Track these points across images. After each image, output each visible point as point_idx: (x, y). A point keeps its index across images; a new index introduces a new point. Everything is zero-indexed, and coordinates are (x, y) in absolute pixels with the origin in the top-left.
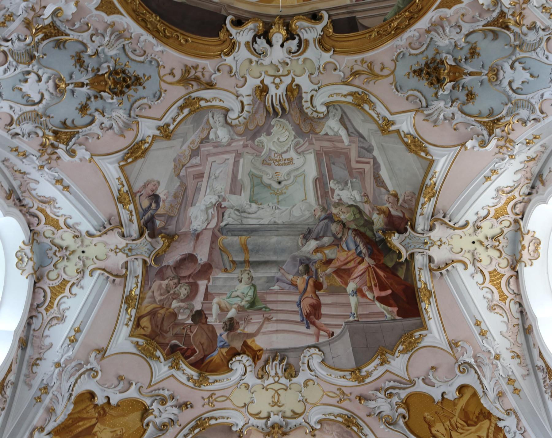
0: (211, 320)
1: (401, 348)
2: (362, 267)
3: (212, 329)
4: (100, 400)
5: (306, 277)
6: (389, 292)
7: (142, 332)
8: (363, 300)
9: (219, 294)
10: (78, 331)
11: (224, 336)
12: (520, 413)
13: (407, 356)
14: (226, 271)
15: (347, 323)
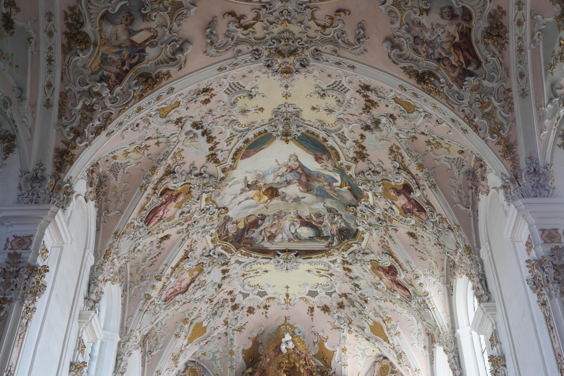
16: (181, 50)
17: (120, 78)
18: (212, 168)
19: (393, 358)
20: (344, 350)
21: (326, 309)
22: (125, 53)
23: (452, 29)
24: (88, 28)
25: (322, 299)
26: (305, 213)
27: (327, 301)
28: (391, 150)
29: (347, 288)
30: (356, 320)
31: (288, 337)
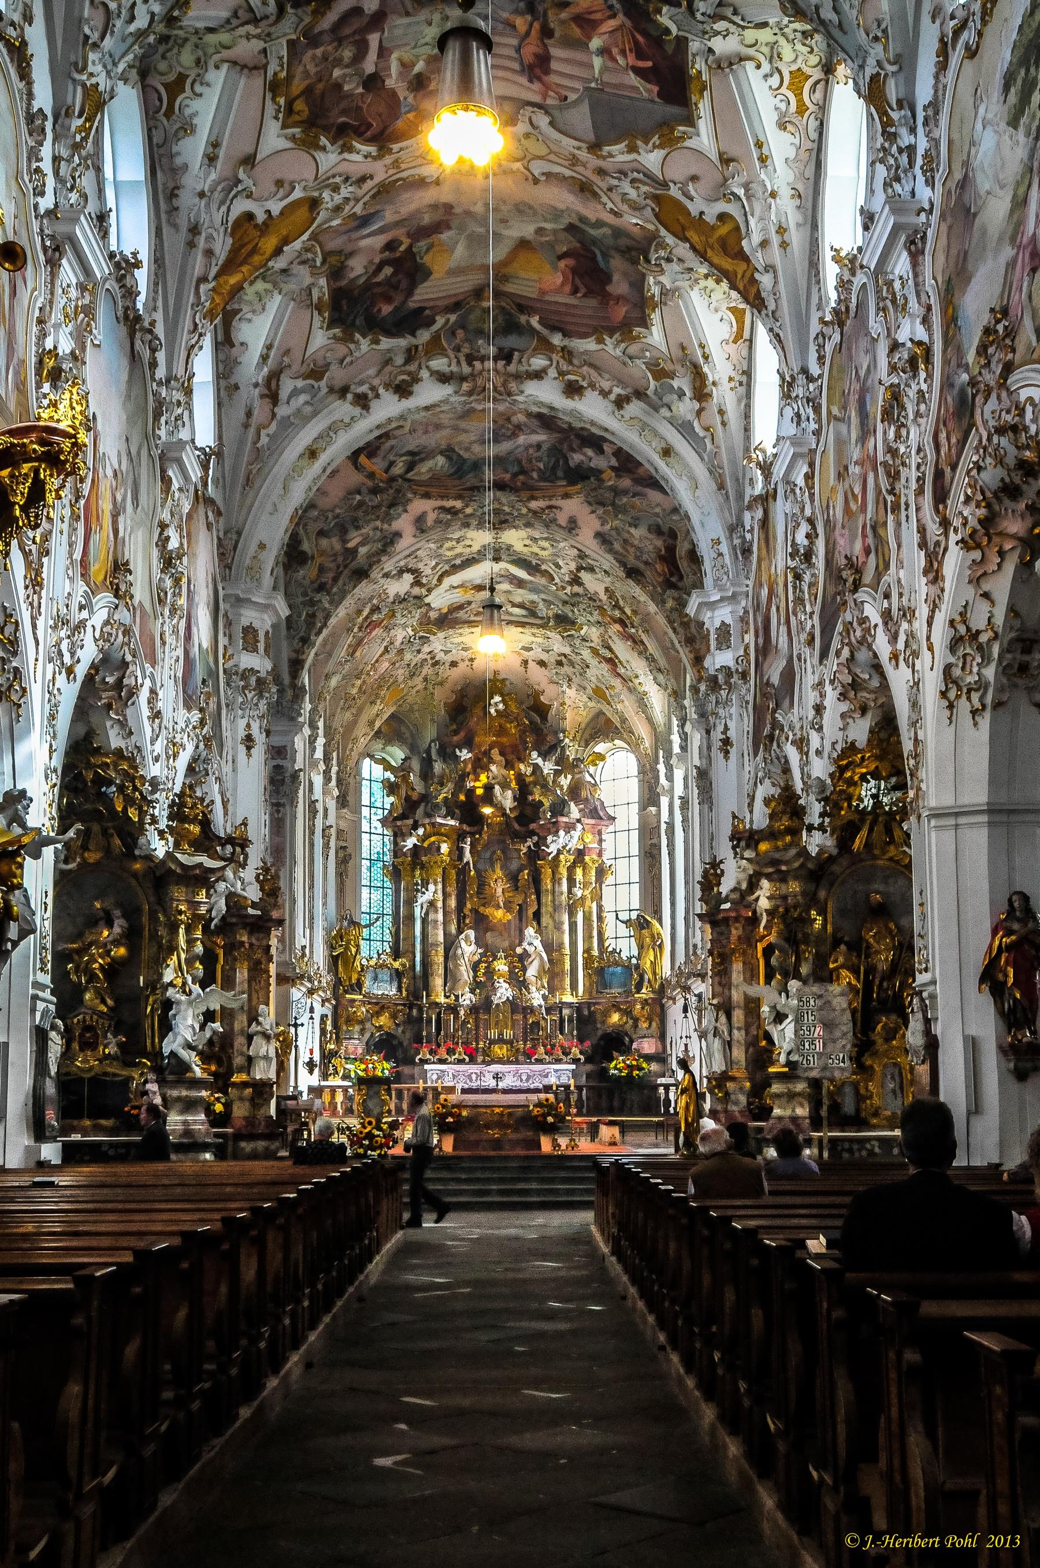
0: (390, 83)
1: (656, 139)
2: (612, 24)
3: (393, 94)
4: (261, 217)
5: (529, 18)
6: (650, 64)
7: (297, 118)
8: (610, 64)
9: (398, 47)
10: (216, 145)
11: (410, 99)
12: (780, 273)
13: (662, 153)
14: (408, 14)
15: (587, 89)
16: (392, 543)
17: (335, 580)
18: (416, 591)
19: (616, 720)
20: (563, 704)
21: (542, 663)
22: (340, 559)
23: (659, 543)
24: (306, 546)
25: (538, 653)
26: (518, 600)
27: (544, 657)
28: (607, 589)
29: (567, 650)
30: (576, 680)
31: (497, 698)
